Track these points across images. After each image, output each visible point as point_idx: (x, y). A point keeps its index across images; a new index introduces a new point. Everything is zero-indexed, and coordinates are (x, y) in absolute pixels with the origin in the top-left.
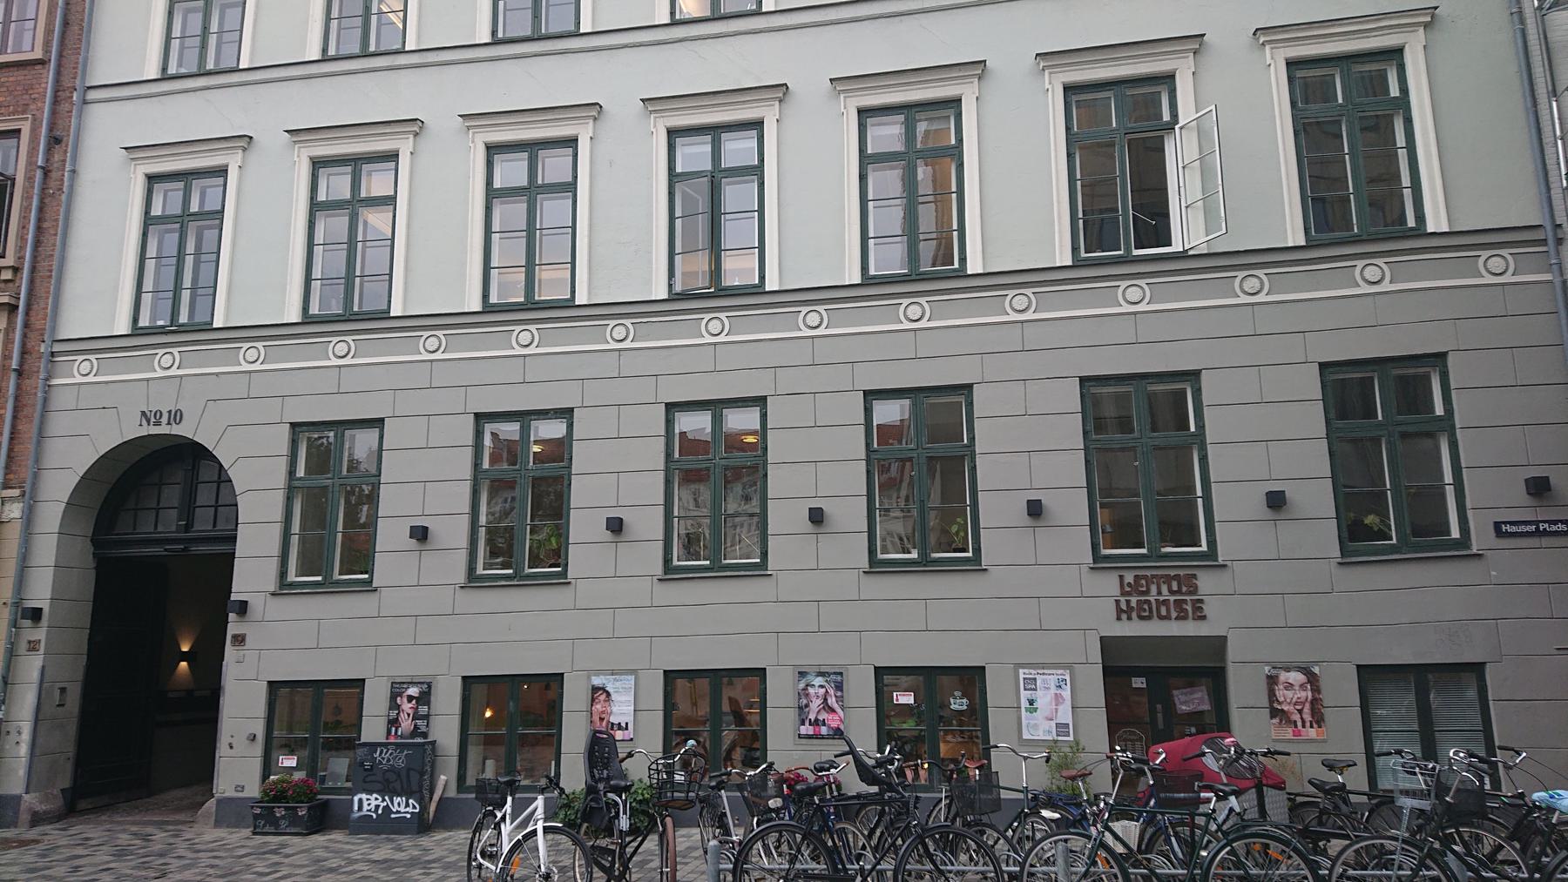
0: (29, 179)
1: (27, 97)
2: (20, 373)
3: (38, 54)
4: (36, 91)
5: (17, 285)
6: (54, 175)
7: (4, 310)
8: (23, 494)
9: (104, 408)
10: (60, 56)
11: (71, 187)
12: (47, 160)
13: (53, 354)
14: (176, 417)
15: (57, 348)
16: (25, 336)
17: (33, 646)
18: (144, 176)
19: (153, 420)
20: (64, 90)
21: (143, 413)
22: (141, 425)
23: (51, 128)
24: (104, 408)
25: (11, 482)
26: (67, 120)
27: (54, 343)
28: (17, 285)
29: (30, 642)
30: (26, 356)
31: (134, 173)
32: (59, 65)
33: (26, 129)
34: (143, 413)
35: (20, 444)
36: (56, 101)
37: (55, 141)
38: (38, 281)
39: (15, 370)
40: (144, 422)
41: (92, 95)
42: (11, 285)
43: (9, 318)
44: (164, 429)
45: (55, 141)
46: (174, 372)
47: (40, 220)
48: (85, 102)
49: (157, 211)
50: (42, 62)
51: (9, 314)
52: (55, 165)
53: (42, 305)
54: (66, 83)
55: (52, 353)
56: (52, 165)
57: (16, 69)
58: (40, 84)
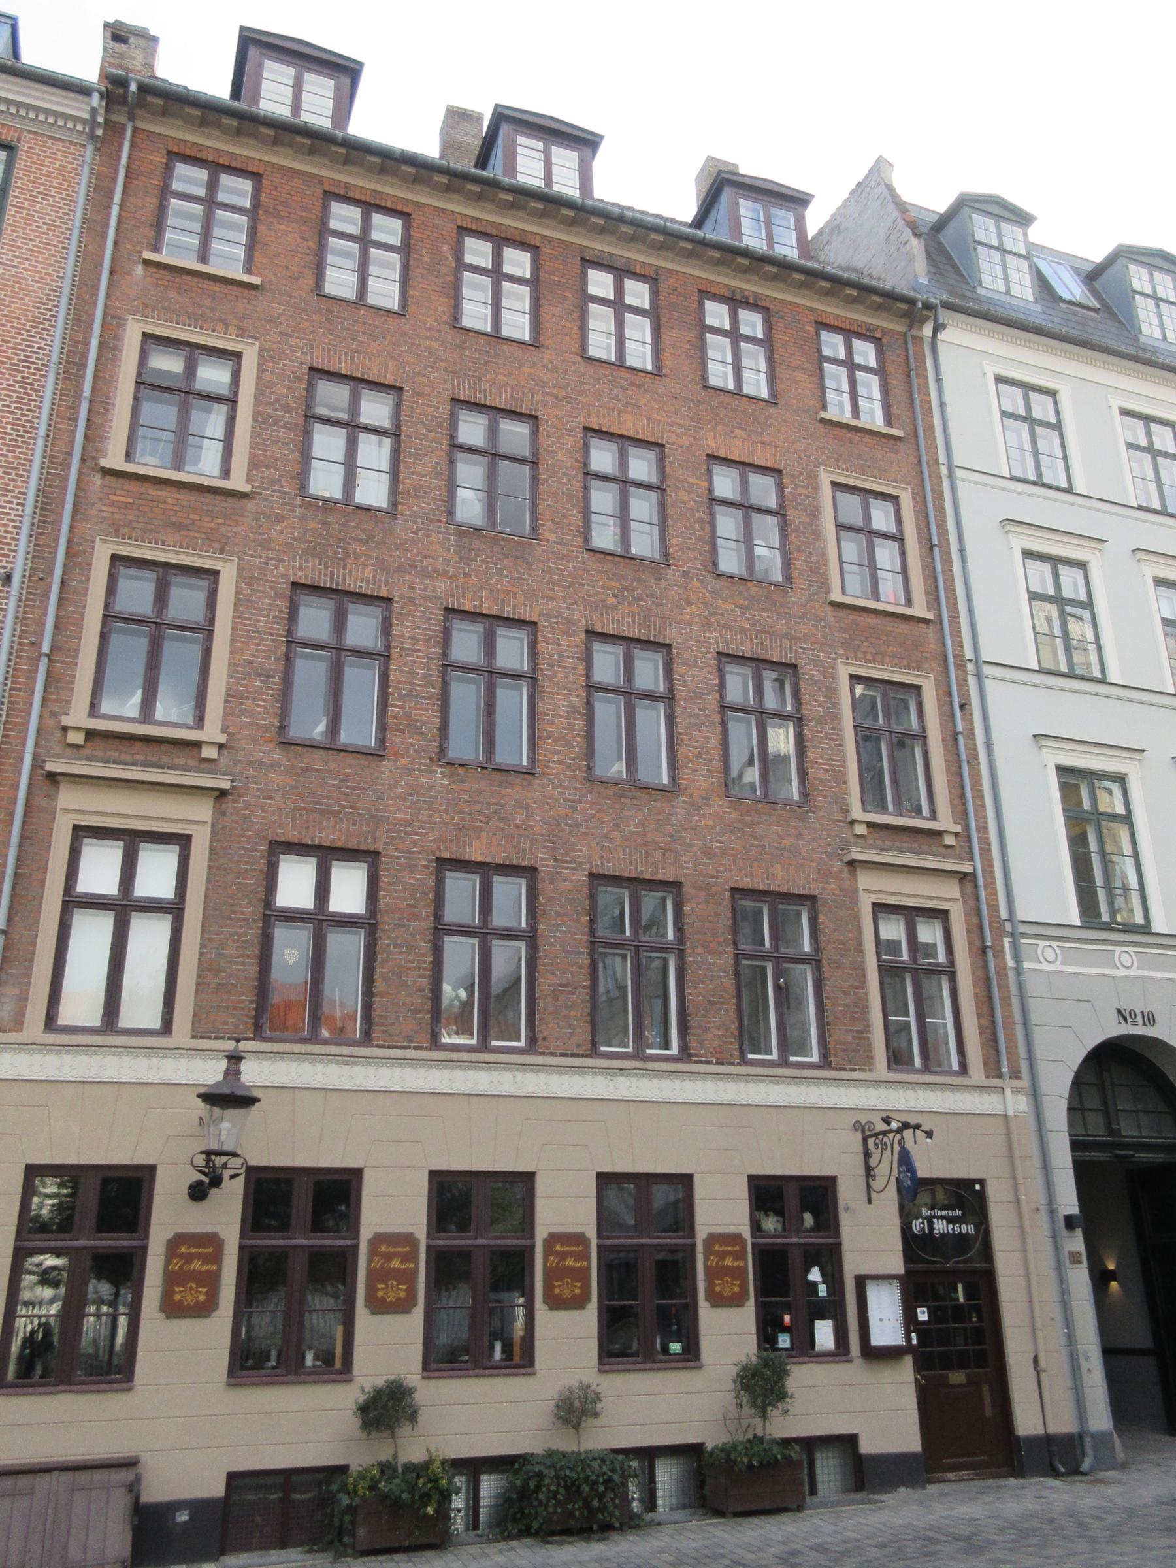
14: (1150, 1019)
17: (1075, 1258)
19: (1129, 1019)
21: (1119, 1011)
34: (1119, 1011)
40: (1122, 1020)
44: (1140, 1030)
46: (1134, 972)
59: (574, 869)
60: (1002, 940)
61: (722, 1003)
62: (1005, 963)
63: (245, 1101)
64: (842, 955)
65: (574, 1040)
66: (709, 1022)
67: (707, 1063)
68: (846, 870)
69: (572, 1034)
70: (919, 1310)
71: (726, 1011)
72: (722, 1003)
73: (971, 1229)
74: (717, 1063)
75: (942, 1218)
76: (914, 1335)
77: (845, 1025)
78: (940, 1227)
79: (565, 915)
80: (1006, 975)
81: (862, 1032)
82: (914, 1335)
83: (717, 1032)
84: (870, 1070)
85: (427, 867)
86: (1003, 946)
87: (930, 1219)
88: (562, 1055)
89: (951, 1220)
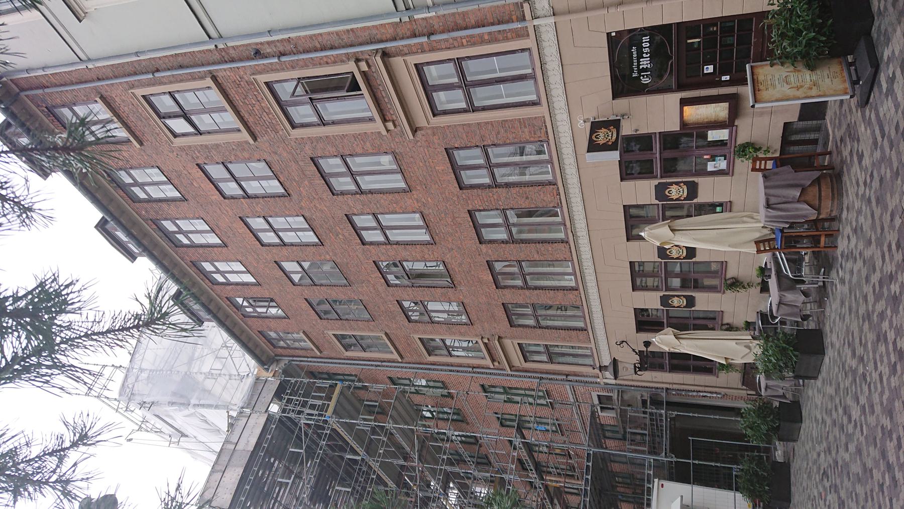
0: (293, 66)
1: (242, 83)
2: (430, 34)
3: (209, 82)
4: (235, 78)
5: (368, 57)
6: (281, 49)
7: (389, 61)
11: (281, 30)
16: (403, 38)
20: (223, 57)
23: (249, 59)
25: (519, 16)
26: (241, 49)
27: (398, 10)
28: (368, 57)
30: (417, 34)
33: (262, 78)
35: (486, 19)
36: (233, 61)
38: (360, 40)
41: (213, 33)
42: (370, 61)
43: (394, 57)
45: (258, 54)
48: (221, 37)
50: (214, 79)
52: (275, 50)
53: (374, 32)
54: (217, 56)
55: (407, 9)
56: (275, 52)
57: (229, 96)
60: (418, 19)
61: (526, 193)
62: (434, 16)
63: (615, 362)
64: (475, 135)
67: (560, 199)
68: (419, 133)
70: (705, 72)
71: (529, 191)
73: (646, 39)
74: (560, 195)
75: (639, 62)
76: (724, 78)
78: (645, 63)
81: (520, 122)
82: (724, 78)
83: (542, 196)
84: (544, 117)
87: (640, 71)
89: (640, 56)
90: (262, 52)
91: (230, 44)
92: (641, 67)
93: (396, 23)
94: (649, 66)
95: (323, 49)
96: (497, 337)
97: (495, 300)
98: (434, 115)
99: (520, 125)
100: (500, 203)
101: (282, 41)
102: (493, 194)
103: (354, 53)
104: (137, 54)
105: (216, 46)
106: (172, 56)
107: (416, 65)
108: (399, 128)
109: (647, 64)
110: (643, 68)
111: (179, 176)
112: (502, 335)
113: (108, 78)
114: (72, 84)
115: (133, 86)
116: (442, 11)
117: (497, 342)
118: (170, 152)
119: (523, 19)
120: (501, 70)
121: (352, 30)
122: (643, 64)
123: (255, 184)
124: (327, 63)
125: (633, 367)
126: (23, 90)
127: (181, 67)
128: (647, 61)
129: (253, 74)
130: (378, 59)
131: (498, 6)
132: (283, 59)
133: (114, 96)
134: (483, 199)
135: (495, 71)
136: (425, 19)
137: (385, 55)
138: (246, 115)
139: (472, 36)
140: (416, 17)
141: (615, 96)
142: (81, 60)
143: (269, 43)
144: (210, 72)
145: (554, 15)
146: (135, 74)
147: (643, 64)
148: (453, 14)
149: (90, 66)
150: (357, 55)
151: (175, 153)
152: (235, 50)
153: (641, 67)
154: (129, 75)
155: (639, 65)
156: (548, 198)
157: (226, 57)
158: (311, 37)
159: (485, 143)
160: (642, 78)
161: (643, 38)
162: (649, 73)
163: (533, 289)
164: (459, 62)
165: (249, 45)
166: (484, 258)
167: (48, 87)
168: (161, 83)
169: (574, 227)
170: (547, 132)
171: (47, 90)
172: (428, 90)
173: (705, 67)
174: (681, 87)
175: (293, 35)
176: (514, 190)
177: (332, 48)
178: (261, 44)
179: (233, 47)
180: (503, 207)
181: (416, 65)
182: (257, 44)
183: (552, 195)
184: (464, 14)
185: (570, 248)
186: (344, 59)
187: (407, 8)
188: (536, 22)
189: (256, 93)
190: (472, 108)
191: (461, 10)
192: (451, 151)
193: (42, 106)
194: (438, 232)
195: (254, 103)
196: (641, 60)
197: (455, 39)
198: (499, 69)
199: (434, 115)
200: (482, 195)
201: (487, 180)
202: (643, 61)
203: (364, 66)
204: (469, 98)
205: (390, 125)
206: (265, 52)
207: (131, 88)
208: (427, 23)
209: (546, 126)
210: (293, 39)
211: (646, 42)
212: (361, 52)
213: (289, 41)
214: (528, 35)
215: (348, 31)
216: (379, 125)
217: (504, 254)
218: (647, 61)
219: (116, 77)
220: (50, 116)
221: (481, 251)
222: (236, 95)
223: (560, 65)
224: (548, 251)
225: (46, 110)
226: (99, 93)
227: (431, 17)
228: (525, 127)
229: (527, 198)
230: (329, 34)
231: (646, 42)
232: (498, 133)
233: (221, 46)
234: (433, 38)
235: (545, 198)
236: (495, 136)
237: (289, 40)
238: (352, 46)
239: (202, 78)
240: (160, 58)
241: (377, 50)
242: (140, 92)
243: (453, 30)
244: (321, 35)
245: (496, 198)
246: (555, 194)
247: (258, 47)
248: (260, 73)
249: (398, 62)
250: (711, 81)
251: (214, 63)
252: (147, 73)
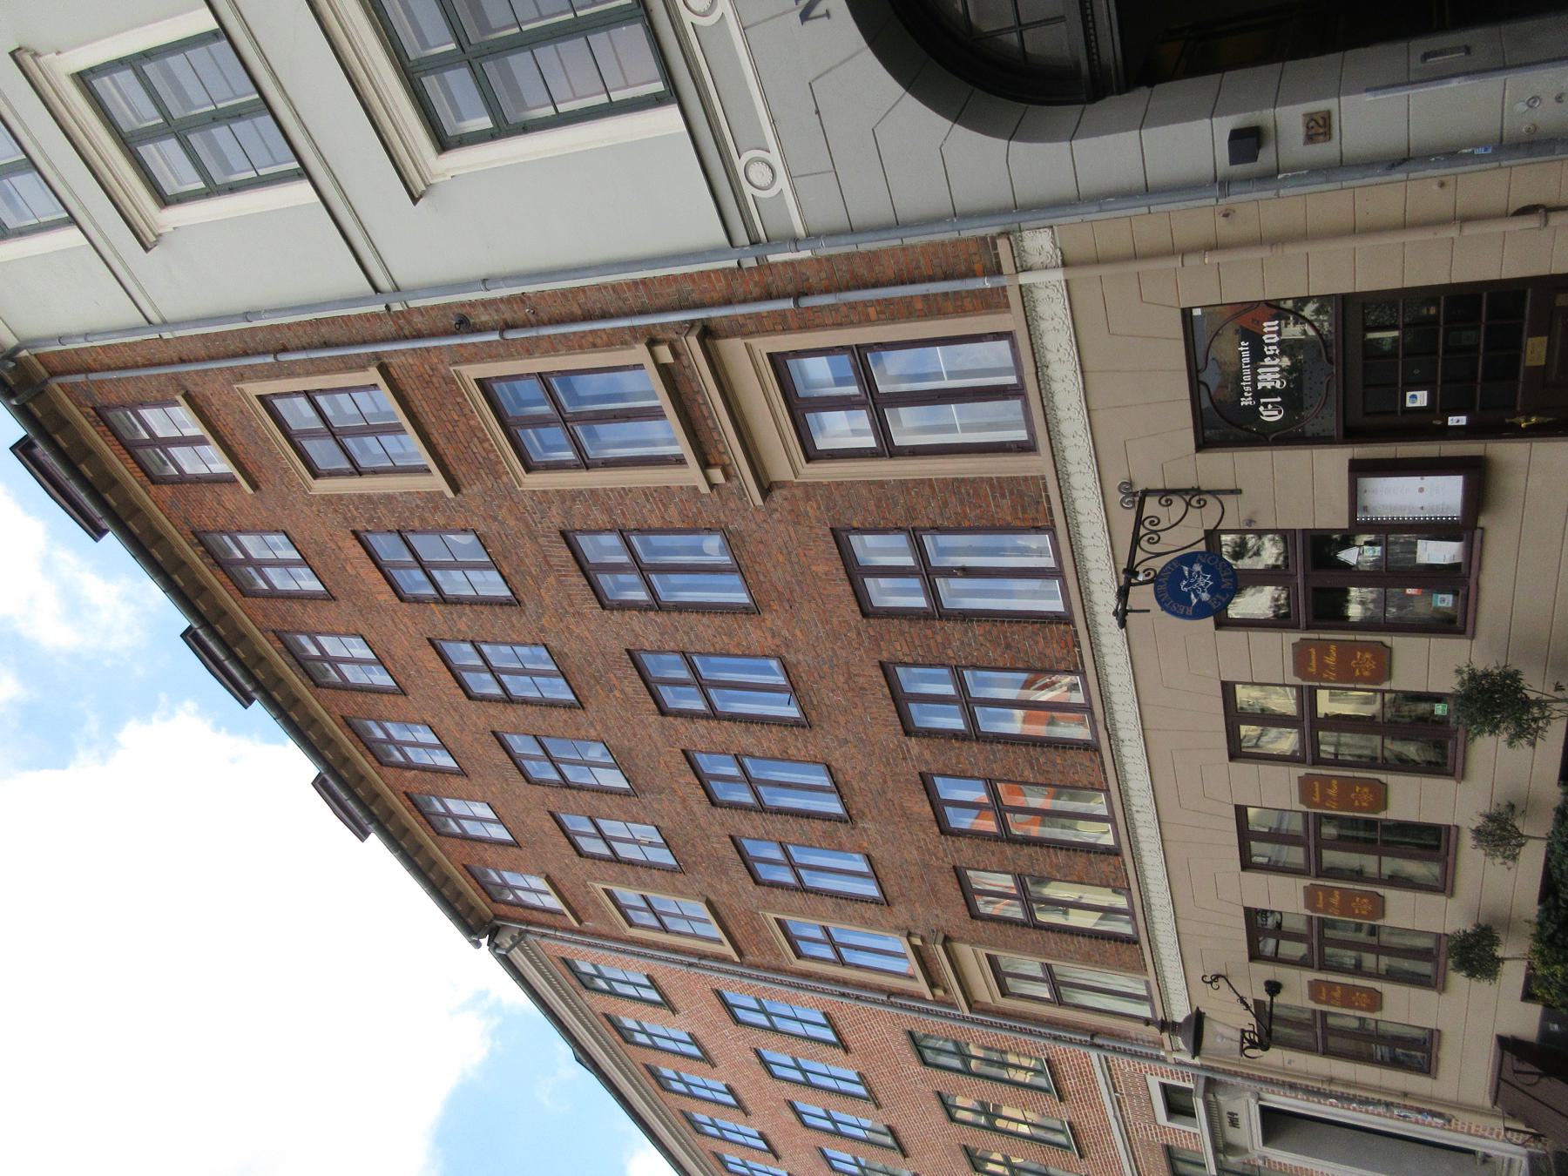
0: (530, 349)
1: (434, 379)
2: (798, 295)
3: (373, 376)
4: (422, 369)
5: (675, 336)
6: (508, 316)
7: (715, 346)
8: (1006, 234)
9: (818, 112)
10: (364, 343)
11: (506, 279)
12: (493, 329)
13: (754, 242)
15: (741, 237)
16: (744, 301)
17: (1319, 127)
18: (442, 156)
20: (402, 329)
22: (828, 14)
23: (446, 333)
24: (818, 112)
25: (989, 265)
26: (433, 314)
27: (735, 244)
28: (675, 336)
29: (1310, 138)
30: (775, 293)
31: (443, 174)
32: (376, 341)
33: (472, 372)
36: (419, 335)
37: (464, 324)
38: (659, 302)
39: (796, 303)
41: (383, 282)
42: (678, 346)
43: (727, 337)
45: (464, 324)
47: (573, 319)
48: (397, 289)
49: (485, 122)
50: (384, 370)
51: (720, 337)
52: (496, 317)
53: (688, 287)
54: (389, 327)
55: (752, 243)
56: (495, 322)
58: (411, 365)
59: (907, 746)
60: (776, 264)
61: (1005, 637)
62: (810, 260)
64: (896, 504)
65: (1088, 764)
66: (1033, 650)
68: (777, 495)
69: (1081, 764)
70: (1409, 404)
71: (1013, 633)
72: (1005, 637)
74: (1079, 647)
75: (1255, 375)
76: (1452, 421)
77: (988, 505)
79: (958, 756)
80: (829, 259)
82: (1452, 421)
84: (1043, 478)
85: (953, 842)
86: (785, 264)
87: (1258, 394)
88: (1105, 773)
90: (472, 321)
91: (413, 304)
92: (1260, 386)
93: (731, 270)
94: (1278, 385)
95: (587, 317)
96: (941, 936)
97: (936, 858)
98: (809, 459)
99: (993, 492)
100: (950, 652)
101: (509, 300)
102: (934, 633)
103: (648, 328)
104: (246, 316)
105: (387, 307)
106: (309, 322)
107: (770, 355)
108: (735, 482)
109: (1274, 380)
110: (1264, 388)
111: (321, 553)
112: (953, 934)
113: (197, 360)
114: (136, 366)
115: (241, 376)
116: (826, 250)
117: (940, 948)
118: (307, 505)
119: (997, 271)
120: (952, 375)
121: (644, 281)
122: (1266, 380)
123: (457, 575)
124: (594, 346)
125: (1238, 1036)
126: (54, 374)
127: (326, 345)
128: (1273, 373)
129: (456, 363)
130: (693, 341)
131: (943, 244)
132: (511, 335)
133: (209, 394)
134: (913, 642)
135: (939, 376)
136: (791, 264)
137: (707, 333)
138: (441, 442)
139: (889, 302)
140: (772, 258)
141: (1203, 444)
142: (150, 322)
143: (486, 304)
144: (377, 356)
145: (1065, 264)
146: (246, 354)
147: (1266, 380)
148: (848, 256)
149: (167, 335)
150: (653, 332)
151: (314, 508)
152: (423, 316)
153: (1260, 386)
154: (235, 356)
155: (1255, 381)
156: (1054, 651)
157: (406, 327)
158: (564, 294)
159: (916, 524)
160: (1261, 409)
161: (1265, 324)
162: (1279, 399)
163: (1021, 844)
164: (861, 357)
165: (449, 305)
166: (914, 766)
167: (96, 371)
168: (289, 371)
169: (1112, 719)
170: (1050, 509)
171: (94, 376)
172: (800, 407)
173: (1409, 394)
174: (1350, 435)
175: (530, 289)
176: (977, 629)
177: (605, 316)
178: (472, 304)
179: (418, 309)
180: (955, 663)
181: (770, 355)
182: (463, 305)
183: (1063, 645)
184: (872, 257)
185: (1102, 763)
186: (628, 338)
187: (754, 240)
188: (1024, 279)
189: (459, 400)
190: (887, 449)
191: (863, 248)
192: (844, 534)
193: (86, 406)
194: (815, 702)
195: (456, 418)
196: (1260, 370)
197: (852, 306)
198: (948, 373)
199: (809, 459)
200: (910, 633)
201: (920, 602)
202: (1265, 373)
203: (665, 355)
204: (881, 429)
205: (717, 475)
206: (477, 320)
207: (238, 381)
208: (795, 272)
209: (1048, 497)
210: (529, 298)
211: (1269, 332)
212: (661, 325)
213: (523, 302)
214: (1008, 306)
215: (635, 283)
216: (692, 474)
217: (958, 763)
218: (1273, 373)
219: (212, 358)
220: (98, 425)
221: (909, 751)
222: (423, 402)
223: (1078, 372)
224: (1054, 764)
225: (93, 413)
226: (184, 387)
227: (801, 262)
228: (1003, 496)
229: (1008, 646)
230: (599, 287)
231: (1269, 332)
232: (945, 504)
233: (397, 307)
234: (806, 302)
235: (1048, 651)
236: (937, 511)
237: (522, 299)
238: (643, 312)
239: (360, 365)
240: (289, 326)
241: (692, 323)
242: (254, 389)
243: (848, 289)
244: (582, 289)
245: (940, 640)
246: (1070, 644)
247: (464, 311)
248: (468, 361)
249: (733, 349)
250: (1424, 426)
251: (385, 340)
252: (265, 353)
